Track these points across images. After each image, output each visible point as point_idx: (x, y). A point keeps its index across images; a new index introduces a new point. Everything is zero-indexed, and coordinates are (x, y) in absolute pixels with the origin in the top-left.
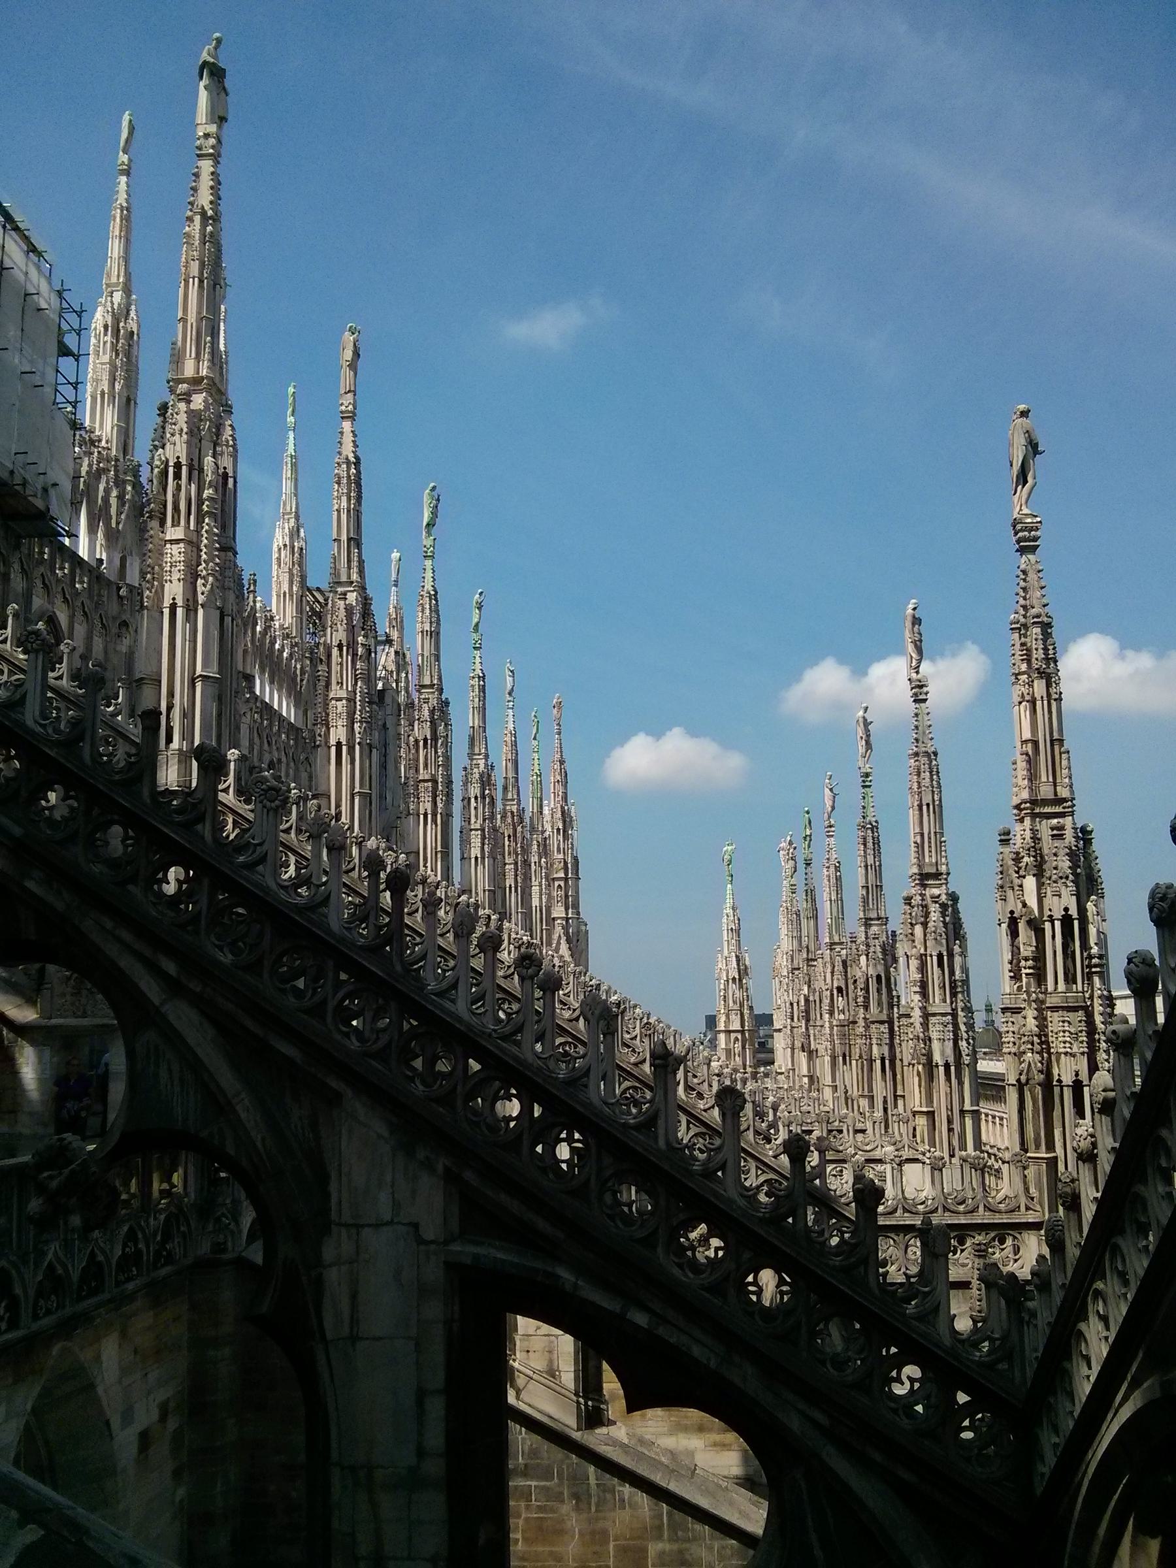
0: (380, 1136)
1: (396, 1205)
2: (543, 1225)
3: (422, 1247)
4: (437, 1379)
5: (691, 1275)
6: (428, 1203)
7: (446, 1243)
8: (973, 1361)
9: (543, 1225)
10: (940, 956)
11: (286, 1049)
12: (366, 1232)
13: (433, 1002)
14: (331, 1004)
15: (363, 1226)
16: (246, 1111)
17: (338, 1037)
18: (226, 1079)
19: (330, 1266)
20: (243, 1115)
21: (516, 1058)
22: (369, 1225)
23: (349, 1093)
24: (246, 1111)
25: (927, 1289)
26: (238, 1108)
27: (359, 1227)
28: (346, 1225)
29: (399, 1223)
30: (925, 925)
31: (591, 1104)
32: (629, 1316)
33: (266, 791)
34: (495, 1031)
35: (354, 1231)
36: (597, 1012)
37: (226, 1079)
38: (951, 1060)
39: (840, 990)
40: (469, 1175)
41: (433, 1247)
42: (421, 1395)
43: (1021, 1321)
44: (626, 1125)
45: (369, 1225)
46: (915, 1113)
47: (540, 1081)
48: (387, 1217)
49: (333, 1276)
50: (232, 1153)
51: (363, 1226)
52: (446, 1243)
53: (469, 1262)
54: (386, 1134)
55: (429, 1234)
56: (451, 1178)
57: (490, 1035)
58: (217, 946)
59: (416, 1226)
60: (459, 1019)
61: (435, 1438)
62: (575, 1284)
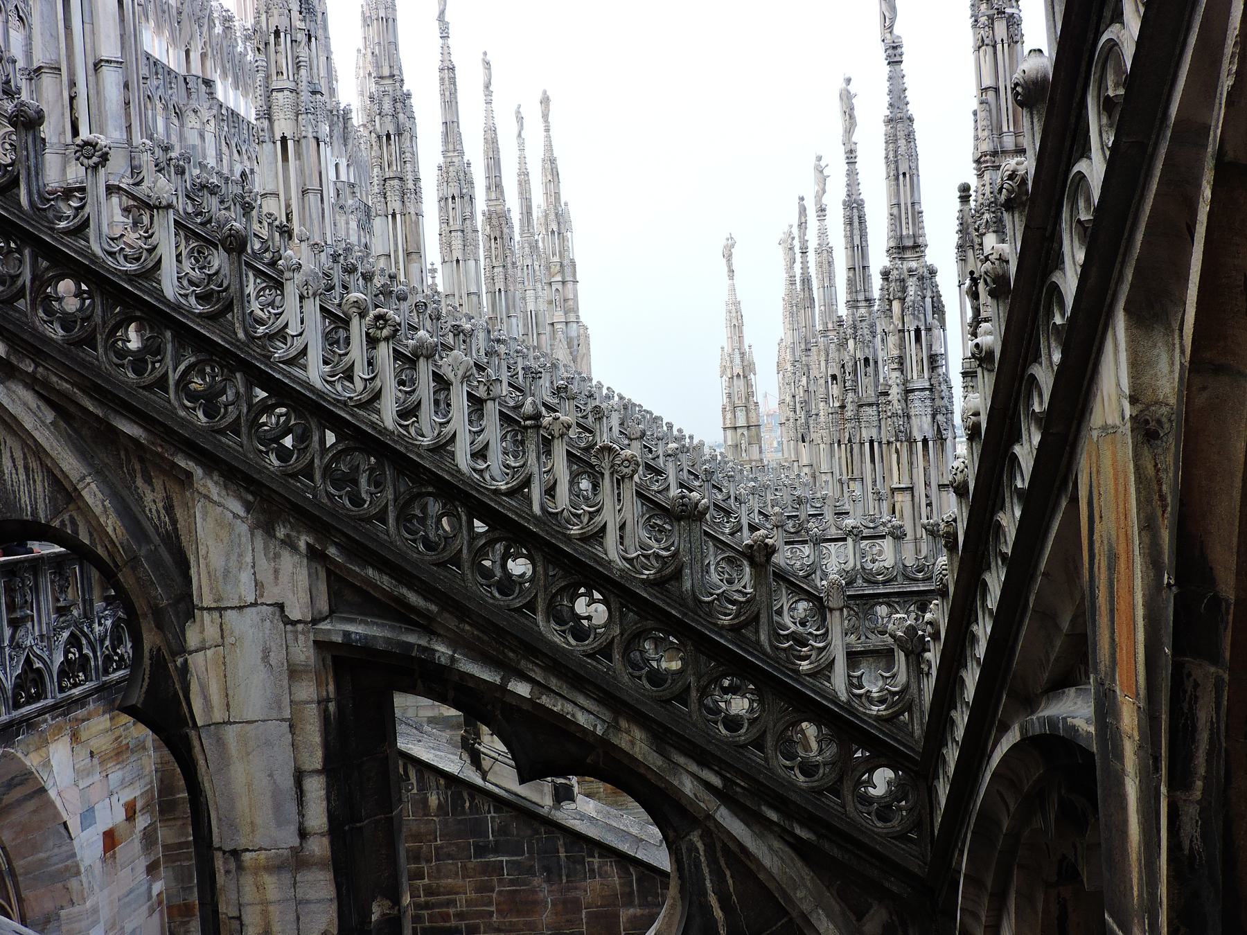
0: (236, 516)
1: (258, 585)
2: (414, 598)
3: (289, 627)
4: (315, 760)
5: (573, 642)
6: (294, 582)
7: (315, 621)
8: (870, 716)
9: (414, 598)
11: (131, 429)
13: (281, 371)
14: (173, 378)
15: (226, 609)
16: (93, 495)
17: (182, 413)
18: (70, 464)
19: (196, 651)
20: (90, 501)
21: (373, 425)
22: (232, 608)
23: (198, 472)
24: (93, 495)
25: (821, 645)
26: (83, 493)
27: (220, 610)
28: (209, 609)
29: (263, 604)
31: (459, 471)
32: (511, 686)
33: (82, 147)
34: (351, 398)
35: (216, 615)
36: (460, 373)
37: (70, 464)
40: (332, 551)
41: (300, 627)
42: (299, 776)
43: (920, 671)
44: (497, 492)
45: (232, 608)
47: (402, 449)
48: (250, 599)
49: (197, 662)
50: (87, 542)
51: (226, 609)
52: (315, 621)
53: (340, 640)
54: (242, 513)
55: (295, 615)
56: (314, 555)
57: (345, 404)
58: (45, 322)
59: (281, 607)
60: (312, 389)
61: (317, 817)
62: (453, 656)
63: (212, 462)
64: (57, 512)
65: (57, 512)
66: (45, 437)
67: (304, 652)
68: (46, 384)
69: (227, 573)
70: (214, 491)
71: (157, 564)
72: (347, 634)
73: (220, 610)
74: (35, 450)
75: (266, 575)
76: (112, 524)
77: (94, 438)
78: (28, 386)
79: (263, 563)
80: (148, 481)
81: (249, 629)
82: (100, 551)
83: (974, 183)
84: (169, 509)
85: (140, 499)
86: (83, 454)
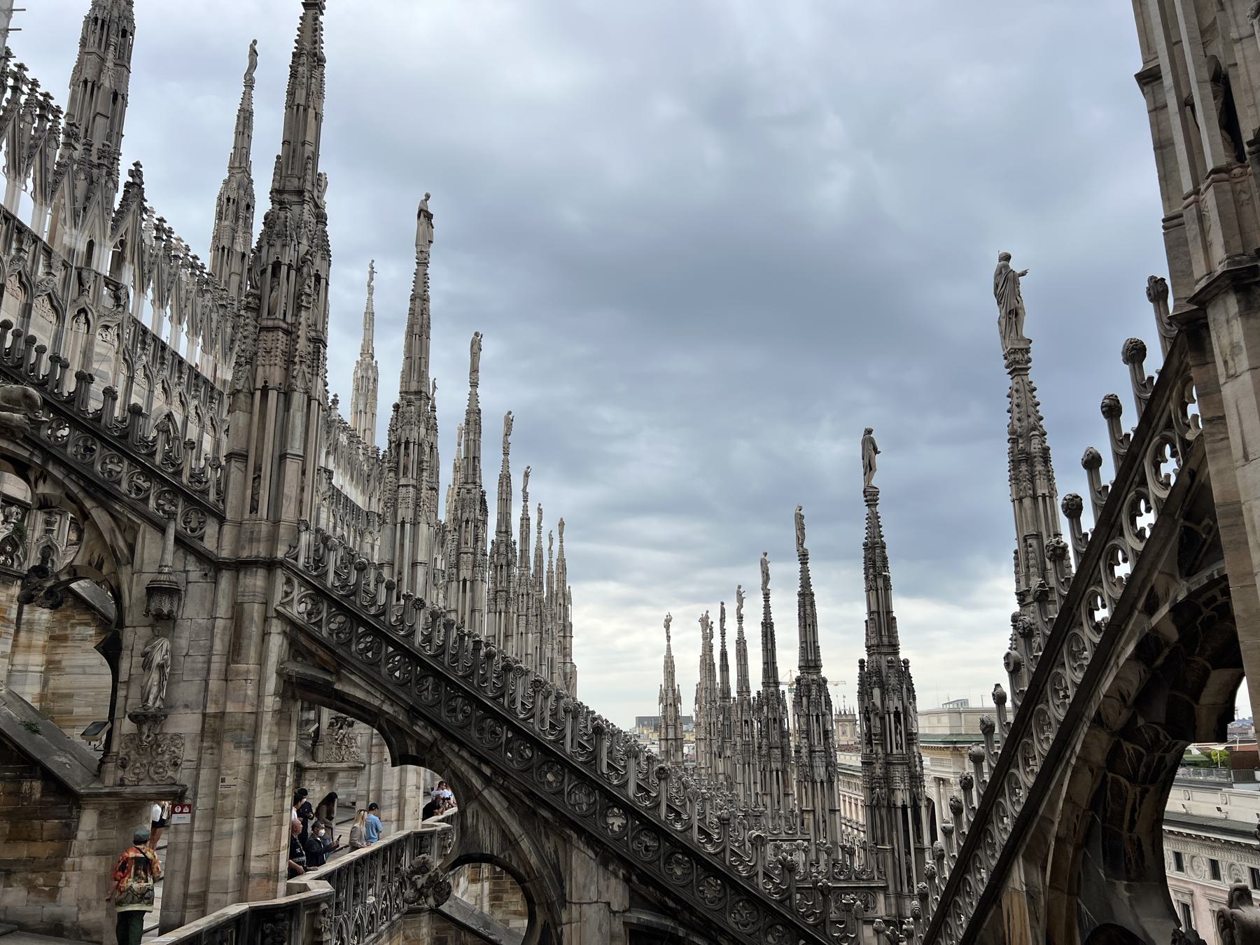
1: (599, 892)
6: (617, 894)
10: (817, 716)
12: (584, 906)
23: (575, 836)
24: (525, 844)
27: (581, 904)
30: (808, 697)
38: (825, 779)
39: (746, 722)
40: (634, 878)
46: (802, 812)
49: (566, 929)
55: (615, 908)
56: (627, 880)
59: (608, 904)
63: (581, 831)
64: (503, 851)
65: (503, 851)
66: (504, 815)
67: (618, 926)
68: (508, 789)
69: (584, 886)
70: (581, 846)
71: (551, 879)
72: (639, 919)
73: (581, 904)
74: (499, 821)
75: (603, 889)
76: (533, 860)
77: (528, 816)
78: (497, 789)
79: (602, 882)
80: (548, 838)
81: (593, 914)
82: (522, 871)
83: (866, 658)
84: (556, 851)
85: (543, 846)
86: (521, 824)
